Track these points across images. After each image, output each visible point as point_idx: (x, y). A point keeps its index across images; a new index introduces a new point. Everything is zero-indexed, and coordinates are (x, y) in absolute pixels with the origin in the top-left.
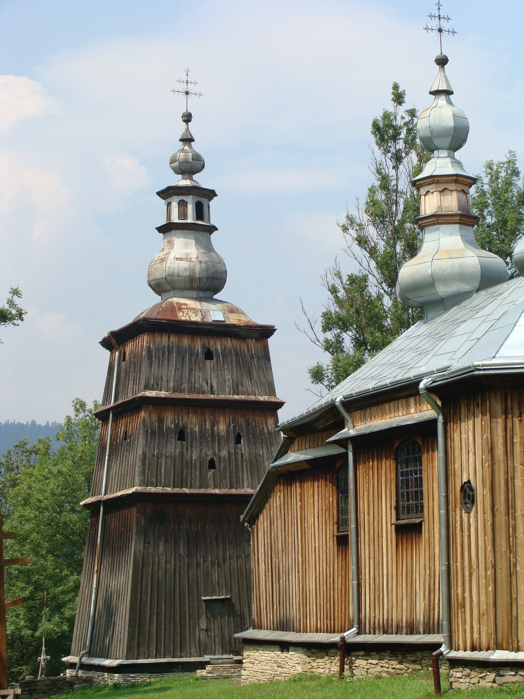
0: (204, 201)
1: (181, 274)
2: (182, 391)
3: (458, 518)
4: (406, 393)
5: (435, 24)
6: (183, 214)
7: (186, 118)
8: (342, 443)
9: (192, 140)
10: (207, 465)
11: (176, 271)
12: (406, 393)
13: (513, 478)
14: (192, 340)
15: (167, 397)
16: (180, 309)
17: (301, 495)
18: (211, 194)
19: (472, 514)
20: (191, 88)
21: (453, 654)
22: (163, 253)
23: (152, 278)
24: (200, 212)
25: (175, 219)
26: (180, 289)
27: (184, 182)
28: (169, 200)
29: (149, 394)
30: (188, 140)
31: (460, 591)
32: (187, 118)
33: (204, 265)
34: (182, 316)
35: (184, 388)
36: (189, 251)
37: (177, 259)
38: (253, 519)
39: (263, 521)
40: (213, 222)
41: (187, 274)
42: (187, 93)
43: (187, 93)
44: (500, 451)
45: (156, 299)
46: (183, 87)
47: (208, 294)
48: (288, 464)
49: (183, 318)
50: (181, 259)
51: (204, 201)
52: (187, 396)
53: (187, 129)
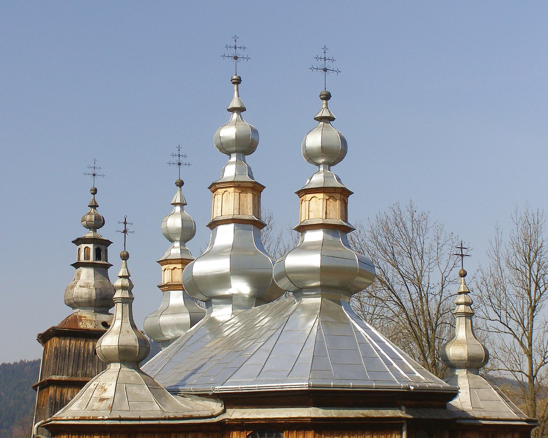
0: (102, 247)
1: (83, 297)
2: (76, 375)
6: (87, 257)
7: (93, 192)
11: (80, 295)
14: (86, 341)
15: (66, 379)
16: (81, 320)
18: (108, 243)
20: (97, 171)
22: (74, 282)
23: (66, 298)
24: (98, 255)
25: (82, 259)
26: (83, 306)
27: (90, 234)
28: (79, 246)
29: (54, 378)
30: (94, 206)
32: (95, 192)
33: (98, 291)
34: (82, 326)
35: (79, 374)
36: (89, 281)
37: (81, 286)
40: (110, 262)
41: (87, 296)
42: (94, 175)
43: (94, 175)
46: (92, 171)
47: (103, 309)
49: (82, 327)
50: (83, 287)
51: (102, 247)
52: (81, 379)
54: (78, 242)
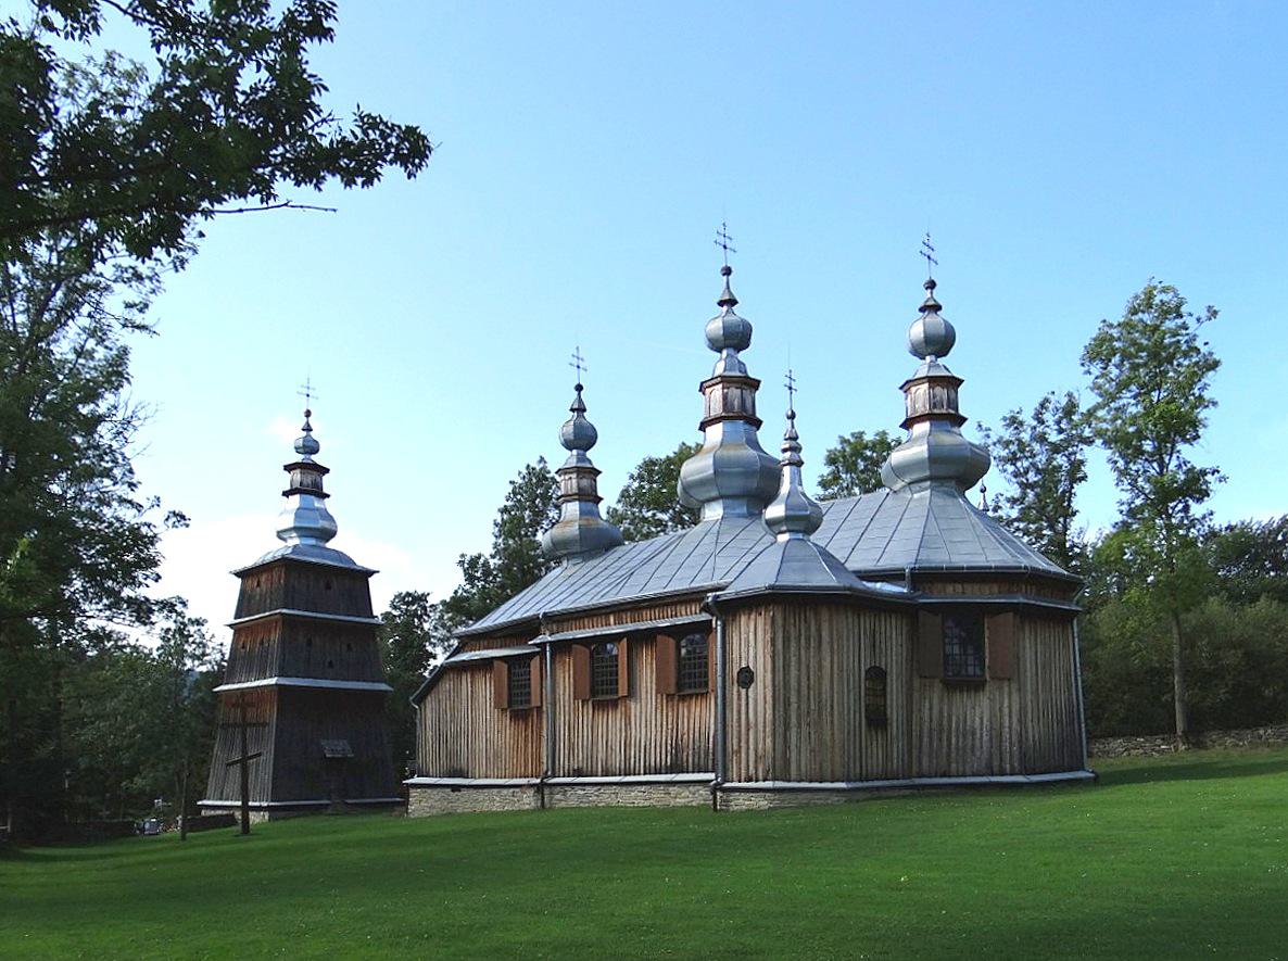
3: (735, 693)
4: (608, 611)
5: (575, 361)
8: (542, 645)
9: (311, 430)
10: (327, 664)
12: (608, 611)
13: (789, 666)
17: (472, 683)
19: (751, 690)
21: (727, 785)
30: (308, 429)
31: (735, 741)
32: (308, 414)
38: (421, 700)
39: (430, 702)
40: (325, 490)
44: (780, 646)
45: (282, 544)
46: (305, 391)
48: (464, 661)
53: (308, 423)
54: (289, 468)
